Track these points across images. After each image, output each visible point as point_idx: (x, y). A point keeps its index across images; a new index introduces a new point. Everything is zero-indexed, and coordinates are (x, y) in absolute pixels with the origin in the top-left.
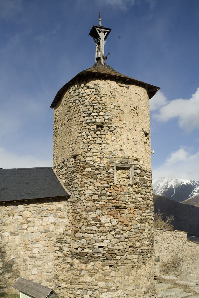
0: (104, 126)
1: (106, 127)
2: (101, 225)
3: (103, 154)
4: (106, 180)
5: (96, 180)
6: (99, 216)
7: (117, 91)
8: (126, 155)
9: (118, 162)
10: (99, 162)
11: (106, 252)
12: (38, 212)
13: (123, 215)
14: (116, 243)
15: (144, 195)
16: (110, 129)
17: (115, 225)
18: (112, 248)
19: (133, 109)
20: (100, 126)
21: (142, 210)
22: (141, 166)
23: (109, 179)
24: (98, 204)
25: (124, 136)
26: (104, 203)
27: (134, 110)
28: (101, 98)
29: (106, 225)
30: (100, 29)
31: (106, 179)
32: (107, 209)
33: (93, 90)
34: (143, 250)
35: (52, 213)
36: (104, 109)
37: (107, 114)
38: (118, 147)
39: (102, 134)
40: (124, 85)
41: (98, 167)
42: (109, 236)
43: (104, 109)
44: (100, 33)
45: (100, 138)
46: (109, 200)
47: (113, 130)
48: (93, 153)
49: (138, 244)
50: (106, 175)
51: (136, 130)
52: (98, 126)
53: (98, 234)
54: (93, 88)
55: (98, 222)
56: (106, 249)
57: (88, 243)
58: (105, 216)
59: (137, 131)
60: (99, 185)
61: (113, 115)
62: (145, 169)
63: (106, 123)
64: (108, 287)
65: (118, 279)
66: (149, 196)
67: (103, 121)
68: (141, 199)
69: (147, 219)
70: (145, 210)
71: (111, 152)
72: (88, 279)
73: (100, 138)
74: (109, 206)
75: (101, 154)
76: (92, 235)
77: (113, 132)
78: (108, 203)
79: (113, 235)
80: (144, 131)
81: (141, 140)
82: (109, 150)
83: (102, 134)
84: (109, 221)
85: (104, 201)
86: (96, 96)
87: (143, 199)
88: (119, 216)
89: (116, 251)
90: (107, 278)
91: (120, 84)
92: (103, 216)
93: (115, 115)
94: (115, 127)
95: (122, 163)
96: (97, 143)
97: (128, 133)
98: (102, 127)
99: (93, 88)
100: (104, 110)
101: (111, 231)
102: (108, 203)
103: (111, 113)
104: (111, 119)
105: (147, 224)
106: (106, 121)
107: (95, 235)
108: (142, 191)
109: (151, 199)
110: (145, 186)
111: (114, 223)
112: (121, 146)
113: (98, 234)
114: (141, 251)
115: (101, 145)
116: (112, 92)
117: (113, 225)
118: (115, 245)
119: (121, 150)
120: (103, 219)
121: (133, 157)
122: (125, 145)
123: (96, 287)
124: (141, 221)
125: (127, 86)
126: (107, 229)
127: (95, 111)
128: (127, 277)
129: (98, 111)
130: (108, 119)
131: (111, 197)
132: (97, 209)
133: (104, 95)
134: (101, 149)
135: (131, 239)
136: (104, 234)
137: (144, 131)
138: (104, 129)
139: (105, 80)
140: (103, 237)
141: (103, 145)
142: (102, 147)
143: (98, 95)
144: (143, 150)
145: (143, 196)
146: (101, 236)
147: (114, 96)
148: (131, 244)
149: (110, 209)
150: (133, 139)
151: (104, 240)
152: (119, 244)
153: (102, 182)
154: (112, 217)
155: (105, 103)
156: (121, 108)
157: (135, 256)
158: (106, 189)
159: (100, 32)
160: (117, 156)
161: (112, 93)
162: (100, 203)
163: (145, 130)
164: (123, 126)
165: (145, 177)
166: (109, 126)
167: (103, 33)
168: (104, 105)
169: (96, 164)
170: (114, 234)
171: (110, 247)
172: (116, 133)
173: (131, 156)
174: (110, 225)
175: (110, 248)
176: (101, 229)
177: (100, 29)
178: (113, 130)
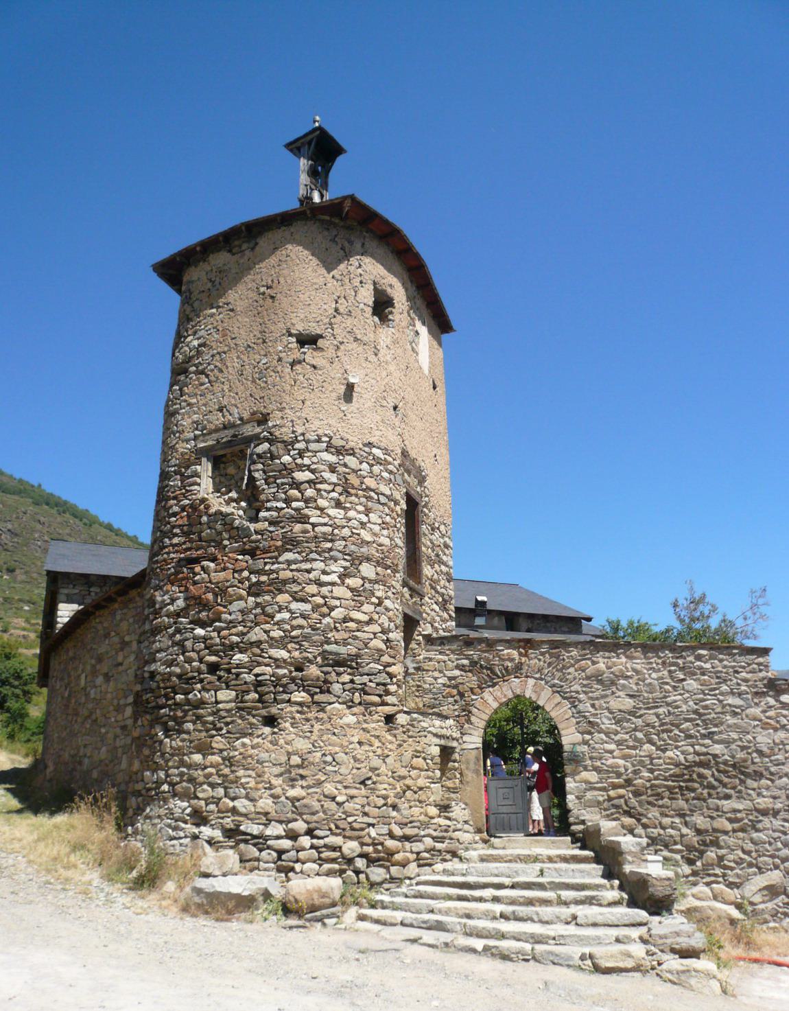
7: (224, 271)
15: (279, 510)
34: (259, 678)
40: (245, 246)
49: (239, 657)
62: (288, 437)
66: (306, 511)
105: (283, 598)
109: (312, 520)
119: (221, 410)
124: (255, 590)
147: (218, 286)
157: (225, 695)
161: (214, 282)
163: (299, 327)
165: (286, 459)
173: (246, 416)
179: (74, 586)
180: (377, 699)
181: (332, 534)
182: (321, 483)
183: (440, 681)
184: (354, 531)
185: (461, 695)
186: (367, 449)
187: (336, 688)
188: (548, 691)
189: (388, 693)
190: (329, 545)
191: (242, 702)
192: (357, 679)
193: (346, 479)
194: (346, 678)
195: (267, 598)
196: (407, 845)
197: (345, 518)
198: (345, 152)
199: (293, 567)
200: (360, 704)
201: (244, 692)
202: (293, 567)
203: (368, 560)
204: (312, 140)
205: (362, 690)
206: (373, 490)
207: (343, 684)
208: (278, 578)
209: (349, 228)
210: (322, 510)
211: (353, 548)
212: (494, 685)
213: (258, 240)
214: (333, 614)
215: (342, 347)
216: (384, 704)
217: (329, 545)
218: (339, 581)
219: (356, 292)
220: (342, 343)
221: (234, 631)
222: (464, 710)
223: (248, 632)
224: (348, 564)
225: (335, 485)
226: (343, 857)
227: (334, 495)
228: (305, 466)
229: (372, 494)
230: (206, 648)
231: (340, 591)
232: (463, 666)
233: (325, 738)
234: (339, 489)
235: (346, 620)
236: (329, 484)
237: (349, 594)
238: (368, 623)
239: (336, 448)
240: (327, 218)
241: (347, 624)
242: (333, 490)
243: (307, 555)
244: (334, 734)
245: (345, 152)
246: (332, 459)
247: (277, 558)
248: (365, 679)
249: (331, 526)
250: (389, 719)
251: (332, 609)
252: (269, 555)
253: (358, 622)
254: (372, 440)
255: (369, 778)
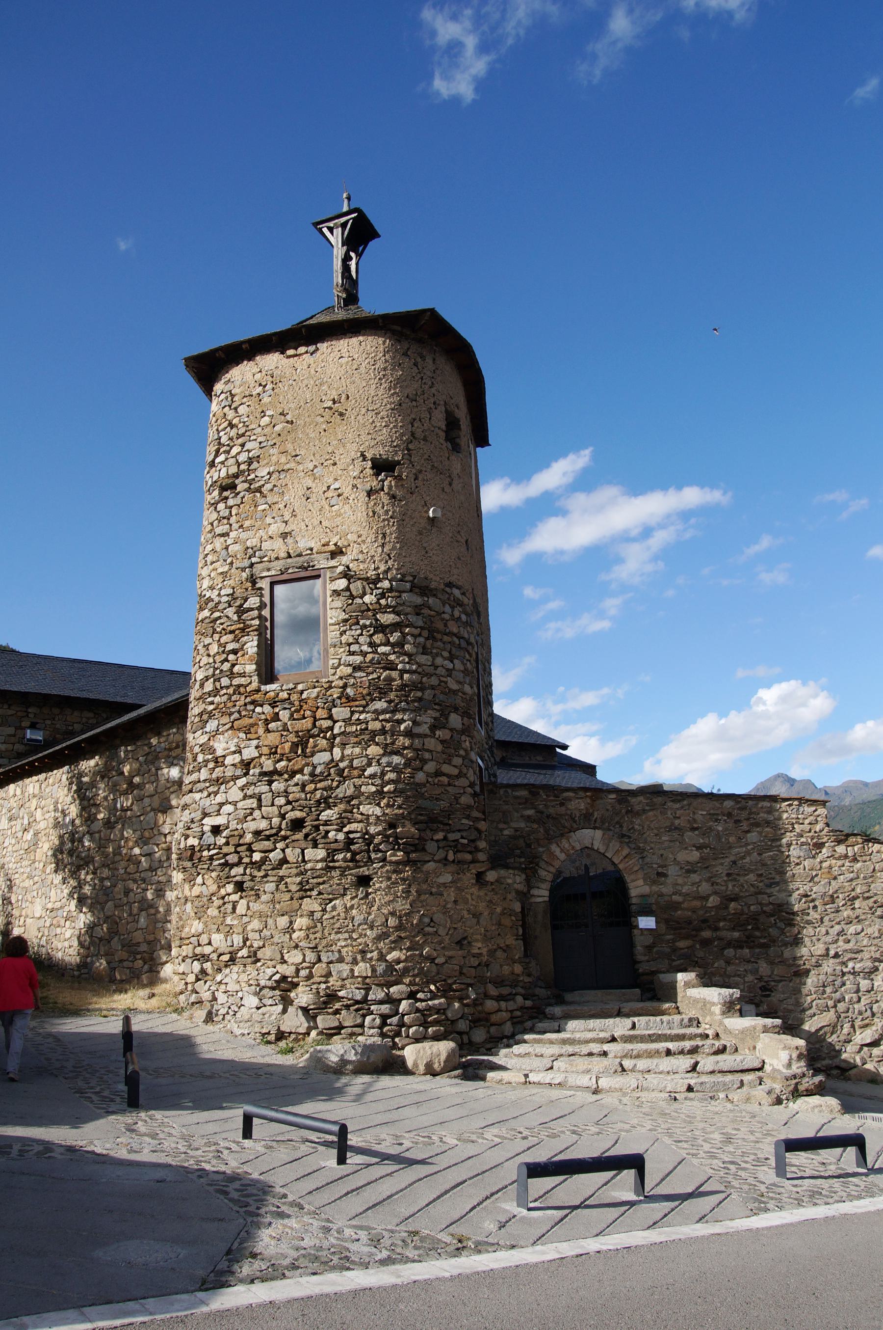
0: (237, 482)
1: (243, 482)
2: (218, 762)
3: (229, 560)
4: (231, 632)
5: (212, 636)
6: (213, 736)
8: (303, 544)
9: (273, 573)
10: (219, 586)
11: (224, 841)
12: (150, 757)
13: (272, 726)
14: (248, 811)
15: (364, 654)
16: (252, 487)
17: (253, 759)
18: (239, 827)
19: (330, 404)
20: (228, 486)
21: (352, 704)
22: (351, 566)
23: (242, 625)
24: (212, 703)
25: (293, 495)
26: (225, 698)
27: (330, 408)
28: (236, 409)
29: (229, 760)
30: (331, 224)
31: (233, 628)
32: (230, 715)
33: (223, 396)
34: (351, 836)
35: (174, 755)
36: (243, 435)
37: (249, 446)
38: (276, 528)
39: (231, 507)
40: (302, 349)
41: (216, 599)
42: (234, 793)
43: (243, 435)
44: (332, 233)
45: (224, 518)
46: (239, 686)
47: (263, 485)
48: (212, 563)
50: (235, 618)
51: (335, 464)
52: (223, 489)
53: (211, 789)
54: (222, 392)
55: (210, 757)
56: (224, 834)
57: (192, 821)
58: (226, 734)
59: (340, 466)
60: (214, 649)
61: (262, 445)
63: (244, 471)
64: (231, 949)
65: (256, 924)
66: (392, 657)
67: (233, 470)
68: (349, 670)
69: (374, 733)
70: (364, 702)
71: (255, 550)
72: (196, 926)
73: (224, 518)
74: (238, 703)
75: (225, 561)
76: (197, 796)
77: (261, 492)
78: (233, 698)
79: (242, 789)
80: (369, 456)
81: (355, 486)
82: (249, 544)
83: (231, 507)
84: (233, 749)
85: (225, 691)
86: (227, 408)
87: (357, 668)
88: (261, 731)
89: (249, 838)
90: (229, 921)
91: (290, 352)
92: (221, 737)
93: (270, 443)
94: (269, 473)
95: (290, 571)
96: (219, 535)
97: (309, 482)
98: (233, 487)
99: (222, 392)
100: (241, 441)
101: (238, 778)
102: (233, 698)
103: (260, 439)
104: (258, 457)
105: (374, 750)
106: (243, 467)
107: (205, 793)
108: (352, 644)
110: (364, 627)
111: (249, 753)
112: (286, 522)
113: (211, 789)
114: (341, 836)
115: (226, 538)
116: (263, 384)
117: (244, 758)
118: (249, 818)
120: (220, 746)
121: (324, 545)
122: (299, 517)
123: (207, 950)
125: (312, 348)
126: (229, 773)
127: (222, 450)
128: (283, 921)
129: (228, 448)
130: (250, 459)
131: (243, 679)
132: (210, 717)
133: (245, 400)
134: (227, 548)
135: (298, 796)
136: (223, 787)
137: (369, 456)
138: (239, 489)
139: (249, 360)
140: (220, 798)
141: (233, 535)
142: (229, 542)
143: (230, 406)
144: (361, 514)
145: (358, 659)
146: (216, 793)
148: (298, 814)
149: (239, 712)
150: (325, 492)
151: (221, 805)
152: (257, 813)
153: (224, 639)
154: (242, 735)
155: (246, 419)
156: (289, 418)
158: (231, 657)
159: (331, 230)
160: (274, 556)
161: (265, 386)
162: (217, 699)
164: (292, 465)
165: (367, 599)
166: (249, 478)
167: (340, 229)
168: (242, 425)
169: (214, 595)
170: (244, 786)
171: (233, 825)
172: (272, 490)
173: (316, 546)
174: (237, 758)
175: (234, 827)
176: (218, 772)
177: (331, 224)
178: (260, 487)
179: (10, 706)
180: (468, 857)
181: (421, 682)
182: (407, 626)
183: (506, 832)
184: (442, 679)
185: (529, 846)
186: (448, 589)
187: (431, 847)
188: (615, 845)
189: (477, 850)
190: (419, 694)
191: (333, 861)
192: (452, 836)
193: (432, 622)
194: (440, 836)
195: (357, 750)
196: (503, 1004)
197: (433, 665)
198: (378, 236)
199: (381, 717)
200: (453, 861)
201: (335, 850)
202: (381, 717)
203: (456, 709)
204: (347, 222)
205: (455, 846)
206: (455, 635)
207: (437, 841)
208: (366, 729)
209: (420, 341)
210: (409, 655)
211: (442, 697)
212: (562, 835)
213: (318, 345)
214: (426, 768)
215: (420, 477)
216: (474, 861)
217: (419, 694)
218: (428, 732)
219: (430, 414)
220: (420, 471)
221: (319, 785)
222: (531, 863)
223: (338, 787)
224: (437, 714)
225: (422, 628)
226: (447, 1019)
227: (422, 640)
228: (390, 607)
229: (455, 639)
230: (289, 803)
231: (431, 743)
232: (529, 817)
233: (423, 897)
234: (425, 633)
235: (438, 773)
236: (416, 628)
237: (440, 748)
238: (458, 777)
239: (420, 588)
240: (398, 328)
241: (440, 778)
242: (420, 635)
243: (397, 704)
244: (431, 893)
245: (378, 236)
246: (419, 600)
247: (364, 707)
248: (457, 836)
249: (419, 673)
250: (479, 876)
251: (424, 761)
252: (357, 703)
253: (448, 776)
254: (453, 579)
255: (465, 938)
